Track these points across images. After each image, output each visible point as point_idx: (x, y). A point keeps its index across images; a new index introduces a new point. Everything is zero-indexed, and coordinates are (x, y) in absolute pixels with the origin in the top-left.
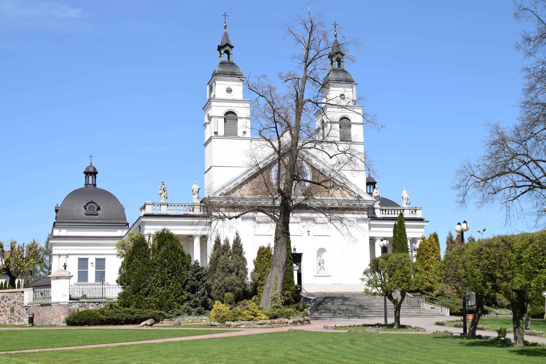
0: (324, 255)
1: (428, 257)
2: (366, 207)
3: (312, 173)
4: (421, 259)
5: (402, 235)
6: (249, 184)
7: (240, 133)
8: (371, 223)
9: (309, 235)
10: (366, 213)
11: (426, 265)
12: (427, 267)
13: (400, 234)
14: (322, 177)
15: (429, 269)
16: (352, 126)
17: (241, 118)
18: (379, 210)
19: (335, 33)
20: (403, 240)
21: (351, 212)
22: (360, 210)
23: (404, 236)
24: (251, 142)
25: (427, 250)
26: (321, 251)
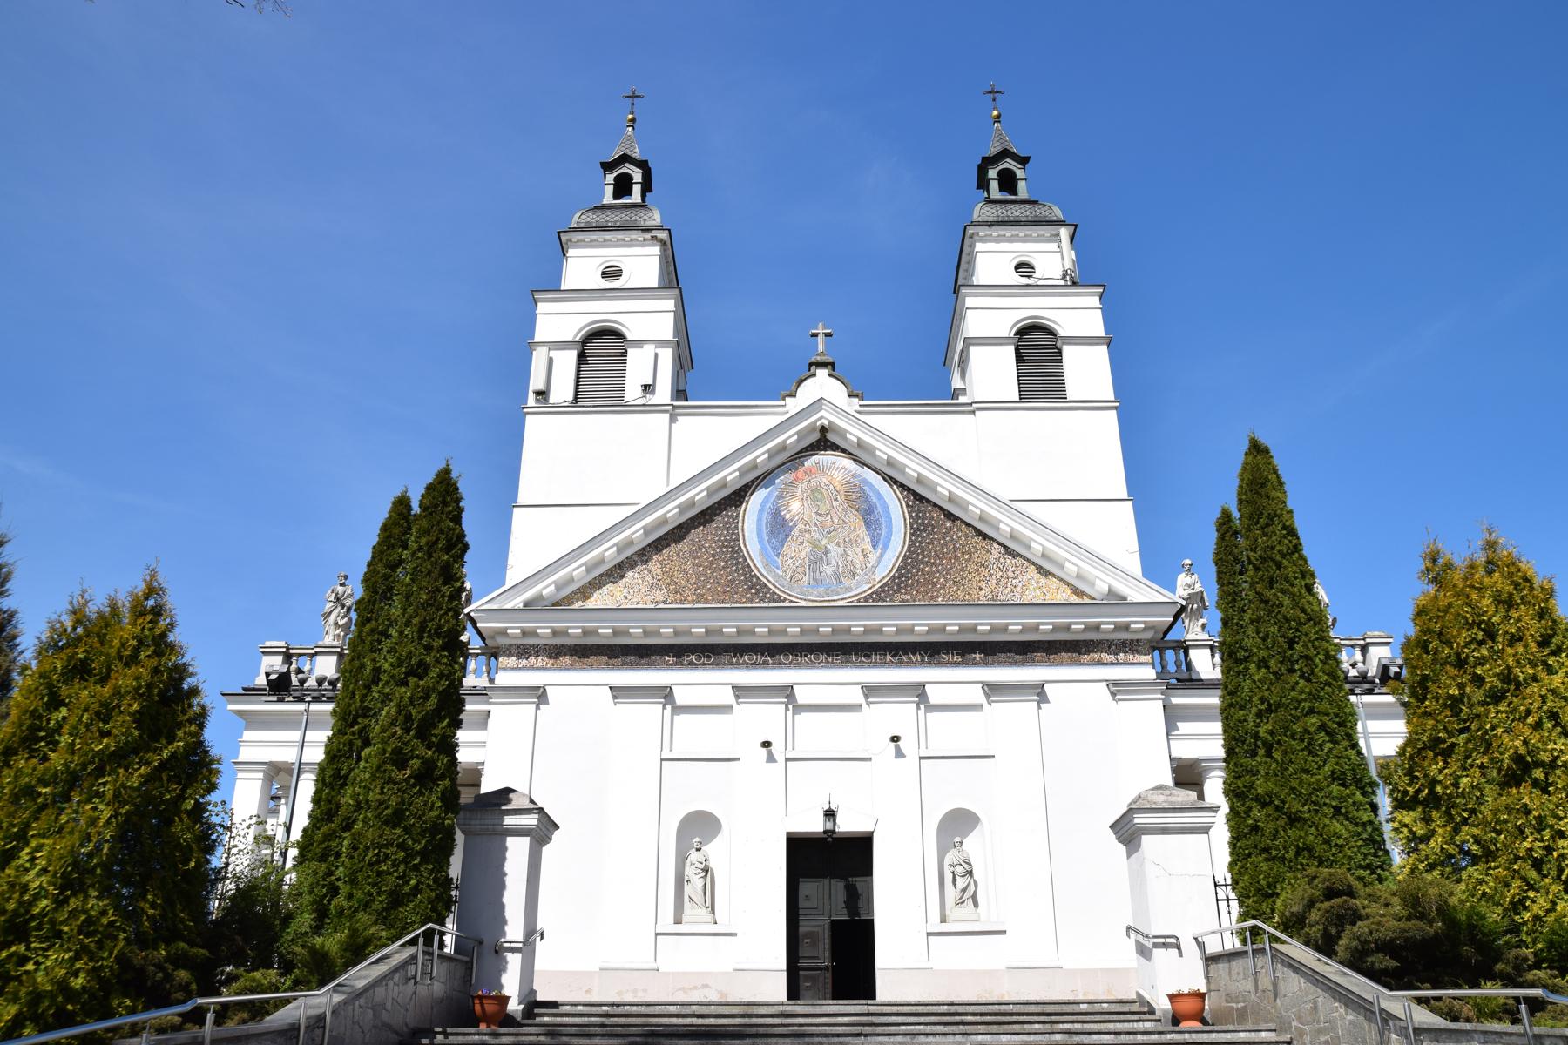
0: (972, 845)
1: (1507, 677)
2: (1148, 635)
3: (910, 517)
4: (1454, 704)
5: (1279, 566)
6: (654, 564)
7: (632, 392)
8: (1175, 700)
9: (899, 754)
10: (1147, 658)
11: (1512, 744)
12: (1518, 758)
13: (1263, 560)
14: (951, 529)
15: (1538, 773)
16: (1067, 350)
17: (639, 343)
18: (1208, 651)
19: (995, 113)
20: (1286, 600)
21: (1086, 658)
22: (1121, 646)
23: (1291, 570)
24: (673, 419)
25: (1491, 634)
26: (958, 823)
